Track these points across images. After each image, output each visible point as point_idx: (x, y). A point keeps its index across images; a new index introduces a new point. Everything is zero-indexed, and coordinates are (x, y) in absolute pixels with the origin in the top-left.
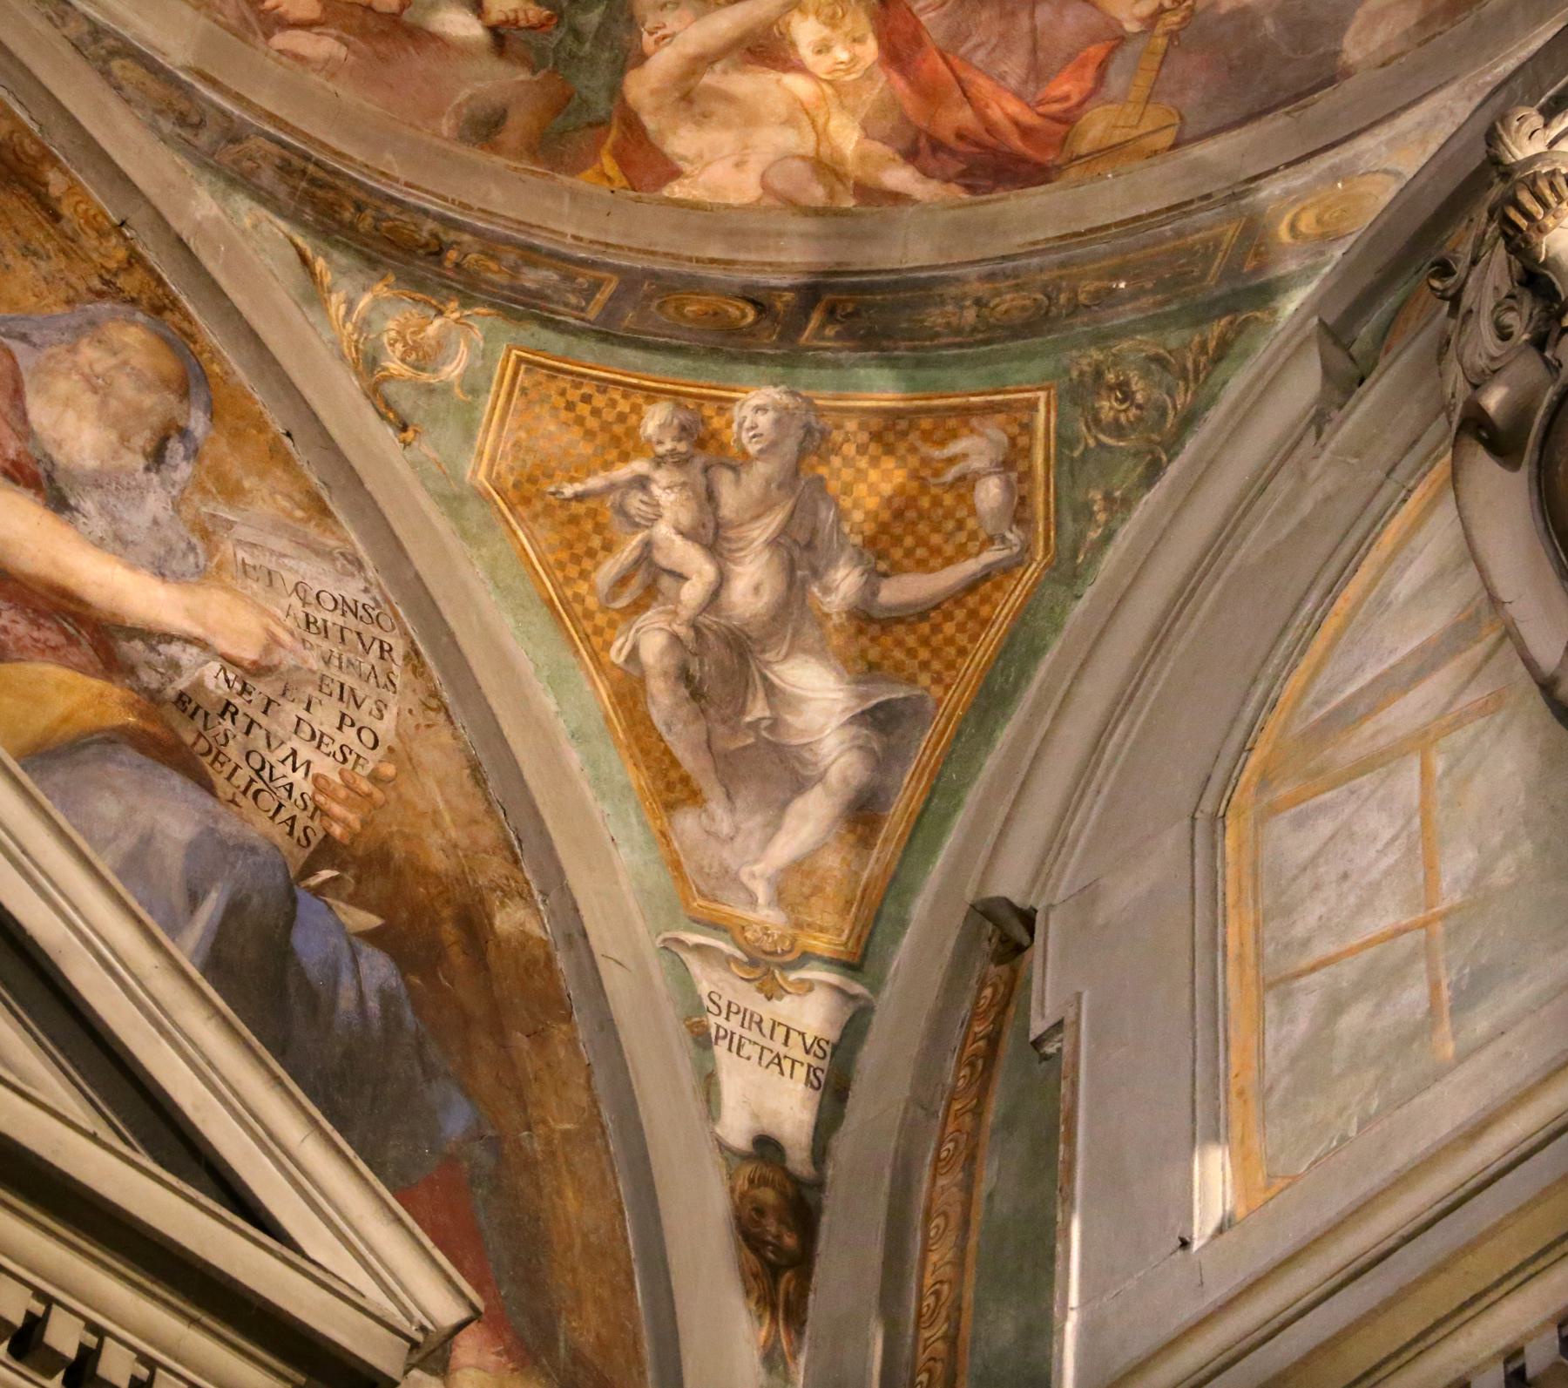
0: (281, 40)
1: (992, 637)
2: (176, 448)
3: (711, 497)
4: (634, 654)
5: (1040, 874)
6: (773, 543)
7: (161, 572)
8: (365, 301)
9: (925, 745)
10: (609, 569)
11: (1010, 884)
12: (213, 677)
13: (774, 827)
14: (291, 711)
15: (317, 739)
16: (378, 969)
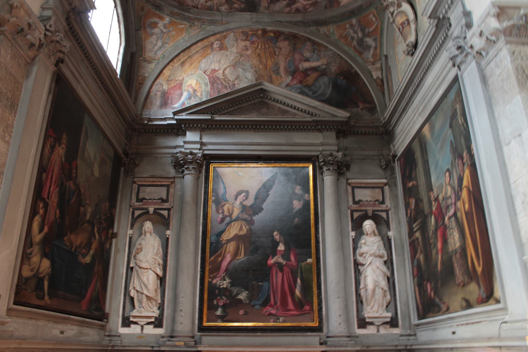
0: (308, 10)
1: (379, 30)
2: (315, 50)
3: (354, 30)
4: (354, 45)
5: (387, 51)
6: (360, 30)
7: (318, 61)
8: (323, 29)
9: (378, 40)
10: (349, 39)
11: (385, 53)
12: (324, 67)
13: (370, 52)
14: (331, 66)
15: (334, 66)
16: (344, 81)
